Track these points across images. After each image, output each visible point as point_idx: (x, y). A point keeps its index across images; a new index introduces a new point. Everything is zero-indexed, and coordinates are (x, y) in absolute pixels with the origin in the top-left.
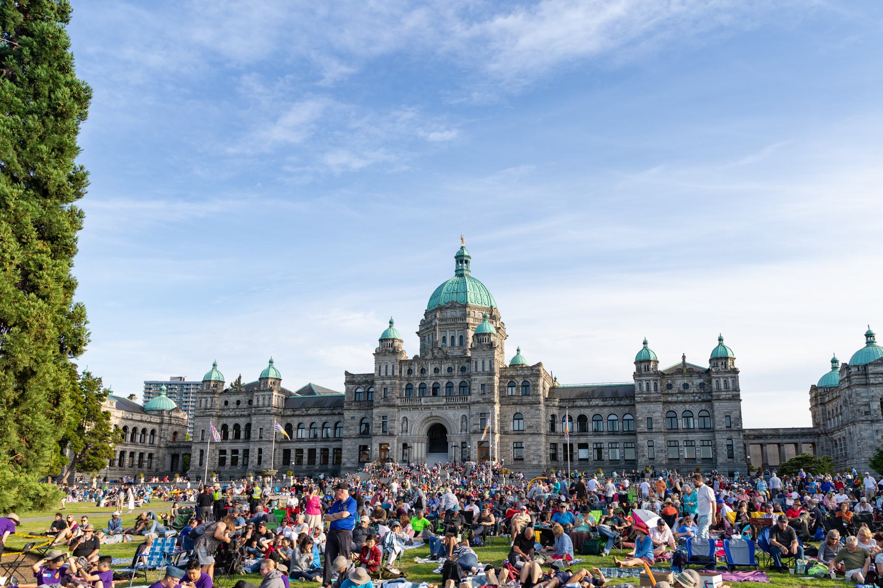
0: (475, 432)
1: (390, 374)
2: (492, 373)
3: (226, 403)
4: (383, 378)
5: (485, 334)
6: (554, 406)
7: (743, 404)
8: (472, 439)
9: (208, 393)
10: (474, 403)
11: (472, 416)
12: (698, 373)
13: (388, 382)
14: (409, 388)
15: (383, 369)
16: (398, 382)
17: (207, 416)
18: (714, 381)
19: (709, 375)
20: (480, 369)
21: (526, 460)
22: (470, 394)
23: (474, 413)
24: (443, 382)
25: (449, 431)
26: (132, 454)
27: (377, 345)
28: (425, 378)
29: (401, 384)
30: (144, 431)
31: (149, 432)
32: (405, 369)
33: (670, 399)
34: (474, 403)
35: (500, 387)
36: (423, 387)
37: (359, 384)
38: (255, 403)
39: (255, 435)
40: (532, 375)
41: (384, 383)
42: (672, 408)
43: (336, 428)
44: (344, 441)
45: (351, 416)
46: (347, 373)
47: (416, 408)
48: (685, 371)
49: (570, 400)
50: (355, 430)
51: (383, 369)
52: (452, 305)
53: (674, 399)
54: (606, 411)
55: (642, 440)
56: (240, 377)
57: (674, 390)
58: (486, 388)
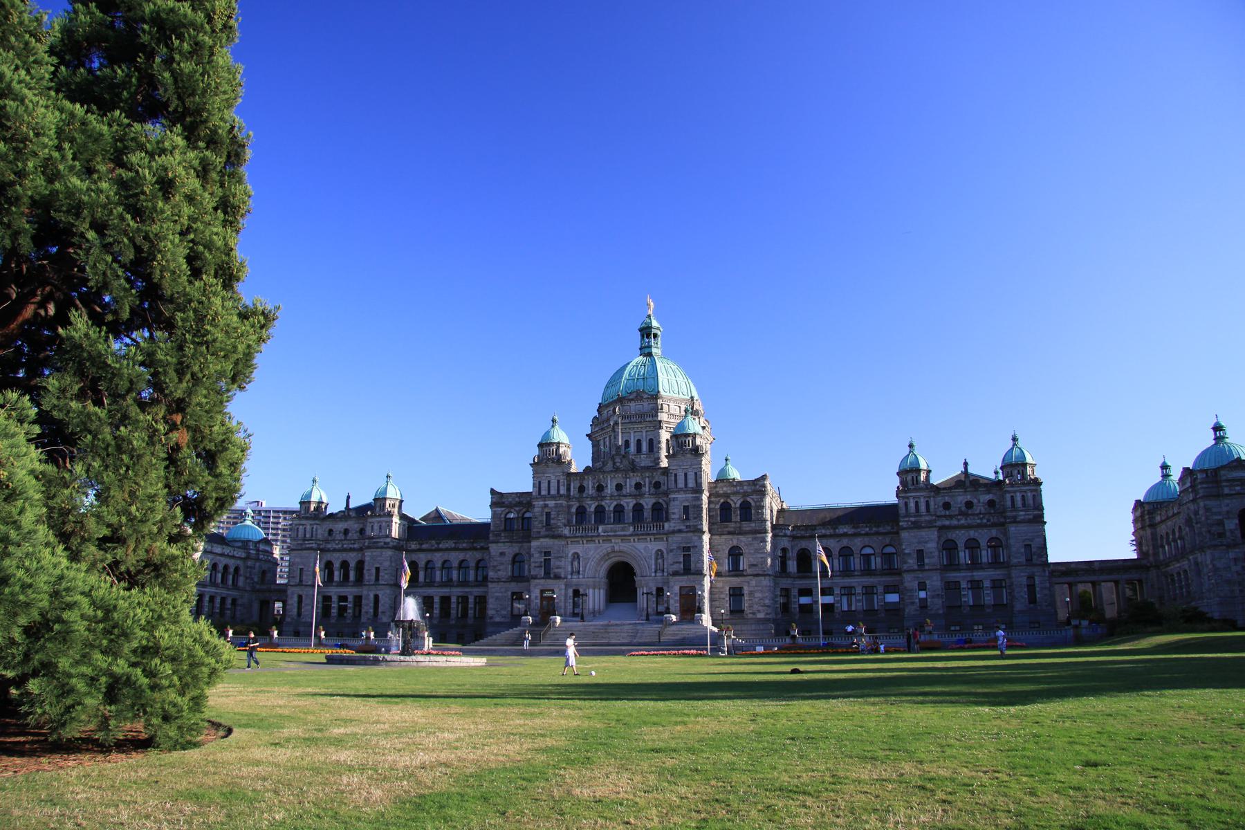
0: (675, 574)
1: (553, 492)
2: (698, 490)
3: (331, 531)
4: (544, 498)
5: (688, 435)
6: (785, 536)
7: (1049, 531)
8: (671, 584)
9: (307, 518)
10: (673, 532)
12: (985, 485)
13: (551, 503)
14: (581, 512)
15: (544, 485)
16: (563, 502)
18: (1008, 496)
19: (1001, 489)
20: (681, 484)
21: (747, 611)
22: (667, 520)
23: (674, 546)
24: (629, 504)
25: (637, 570)
26: (212, 599)
27: (536, 451)
28: (603, 498)
30: (226, 567)
31: (232, 570)
32: (574, 486)
33: (947, 523)
34: (673, 532)
35: (709, 510)
36: (600, 511)
37: (510, 506)
38: (368, 532)
39: (369, 575)
40: (755, 492)
41: (546, 506)
42: (952, 535)
43: (477, 568)
44: (490, 585)
45: (500, 551)
46: (493, 492)
47: (591, 539)
48: (968, 483)
49: (807, 527)
50: (506, 571)
51: (544, 485)
52: (638, 396)
53: (955, 522)
54: (856, 544)
55: (910, 581)
56: (348, 498)
57: (954, 510)
58: (691, 511)
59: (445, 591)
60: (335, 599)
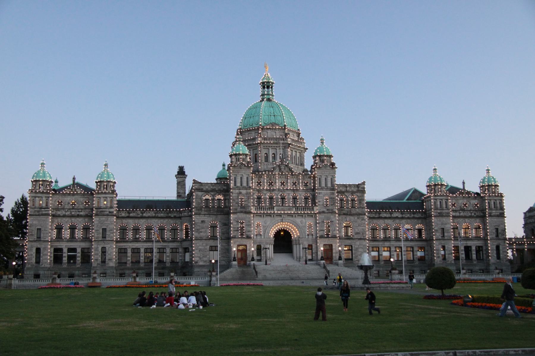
0: (321, 237)
1: (245, 184)
5: (327, 156)
9: (43, 193)
11: (319, 223)
13: (244, 192)
15: (238, 180)
17: (42, 215)
29: (253, 194)
33: (454, 214)
37: (207, 192)
40: (358, 191)
41: (240, 193)
47: (270, 215)
51: (238, 180)
53: (457, 214)
56: (74, 179)
59: (148, 245)
60: (65, 250)
